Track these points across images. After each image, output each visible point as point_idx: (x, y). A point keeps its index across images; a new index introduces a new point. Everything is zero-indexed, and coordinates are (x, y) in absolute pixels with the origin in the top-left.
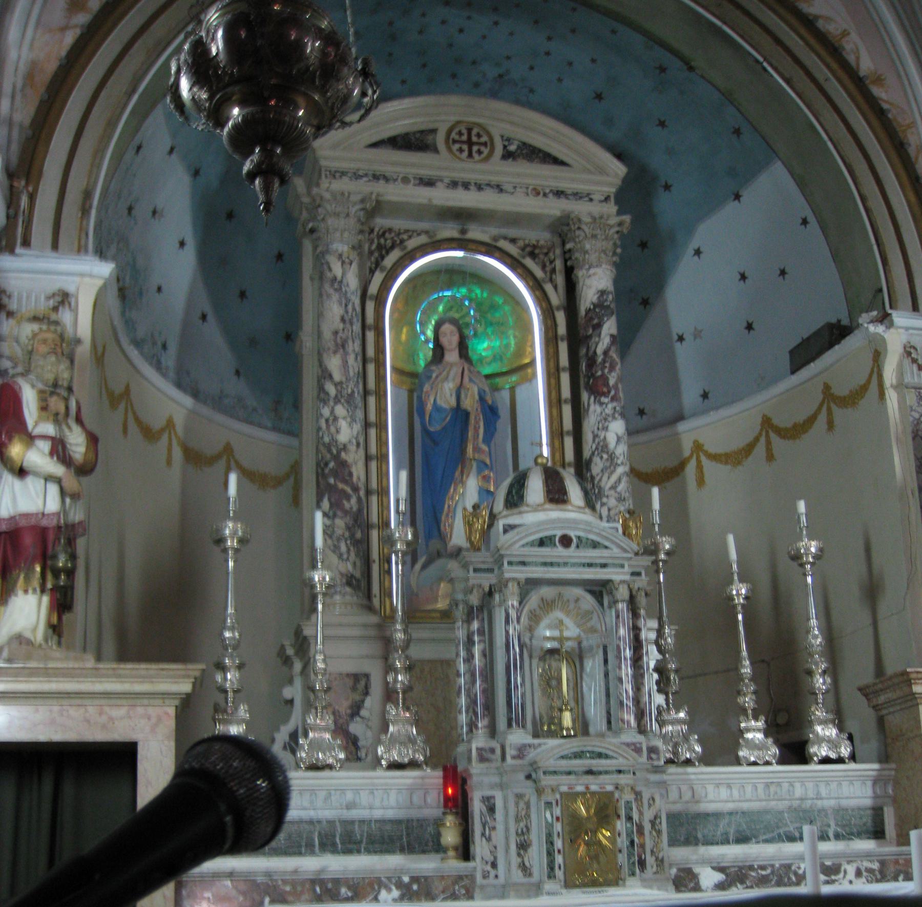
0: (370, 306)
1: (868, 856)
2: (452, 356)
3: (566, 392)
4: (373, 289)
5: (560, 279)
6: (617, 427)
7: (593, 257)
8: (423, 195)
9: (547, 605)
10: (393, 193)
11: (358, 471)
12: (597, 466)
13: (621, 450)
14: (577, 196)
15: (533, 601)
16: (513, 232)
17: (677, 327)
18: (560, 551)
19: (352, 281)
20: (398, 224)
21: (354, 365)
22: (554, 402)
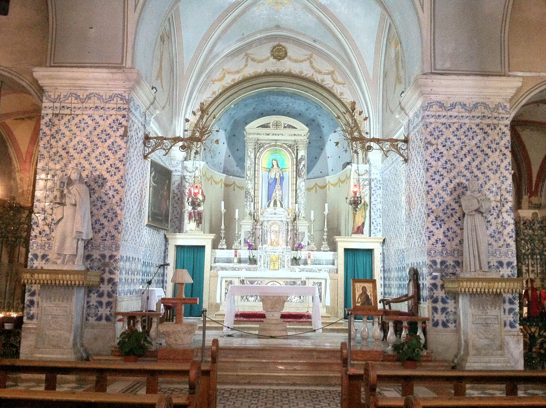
0: (257, 159)
1: (327, 268)
2: (275, 166)
3: (295, 176)
4: (257, 156)
5: (295, 152)
6: (303, 183)
7: (301, 148)
8: (267, 137)
9: (273, 224)
10: (260, 137)
11: (252, 193)
12: (298, 192)
13: (303, 188)
15: (270, 223)
16: (286, 142)
17: (328, 154)
18: (274, 215)
19: (253, 156)
20: (263, 142)
21: (252, 173)
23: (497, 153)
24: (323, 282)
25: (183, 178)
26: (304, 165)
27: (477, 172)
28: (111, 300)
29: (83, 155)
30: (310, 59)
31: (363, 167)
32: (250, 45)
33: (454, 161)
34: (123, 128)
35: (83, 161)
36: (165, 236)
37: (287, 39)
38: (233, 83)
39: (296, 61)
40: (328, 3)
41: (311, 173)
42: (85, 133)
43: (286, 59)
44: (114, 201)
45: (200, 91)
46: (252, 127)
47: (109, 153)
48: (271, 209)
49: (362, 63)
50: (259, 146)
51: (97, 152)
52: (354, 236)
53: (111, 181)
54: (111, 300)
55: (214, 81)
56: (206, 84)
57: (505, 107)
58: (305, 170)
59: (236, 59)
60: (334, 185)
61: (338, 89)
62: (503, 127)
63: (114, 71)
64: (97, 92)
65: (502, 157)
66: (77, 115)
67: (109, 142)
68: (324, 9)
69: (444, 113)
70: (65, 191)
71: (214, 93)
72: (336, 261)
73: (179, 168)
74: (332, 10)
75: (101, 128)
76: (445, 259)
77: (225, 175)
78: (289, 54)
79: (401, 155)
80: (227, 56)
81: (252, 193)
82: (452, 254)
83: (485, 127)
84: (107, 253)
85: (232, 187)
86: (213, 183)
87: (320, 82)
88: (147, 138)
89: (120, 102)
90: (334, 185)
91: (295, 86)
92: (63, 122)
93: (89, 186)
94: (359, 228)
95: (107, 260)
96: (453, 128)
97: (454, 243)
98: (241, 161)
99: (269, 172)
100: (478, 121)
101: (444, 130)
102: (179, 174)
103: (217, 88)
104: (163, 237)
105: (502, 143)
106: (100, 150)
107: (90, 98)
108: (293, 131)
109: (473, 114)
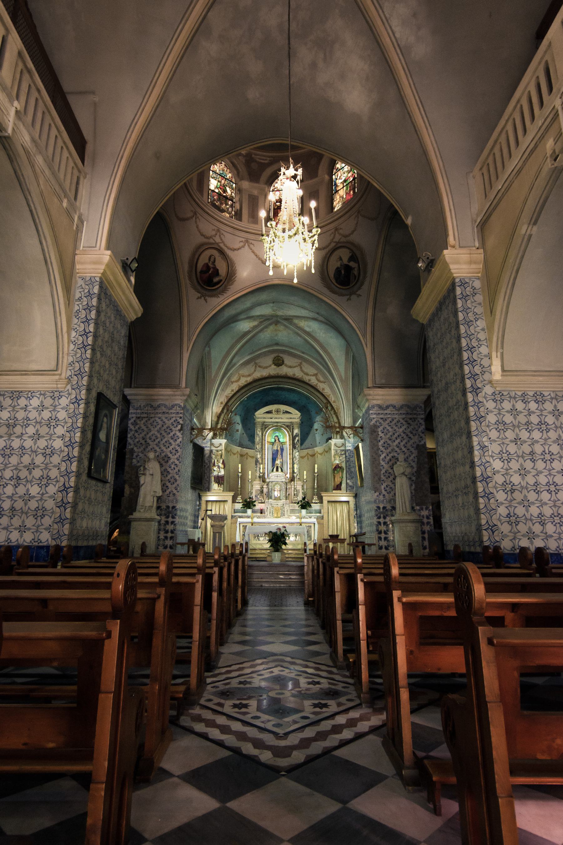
2: (277, 441)
6: (297, 453)
9: (276, 484)
10: (266, 420)
11: (260, 461)
13: (297, 457)
14: (293, 418)
15: (274, 483)
19: (260, 434)
21: (260, 446)
22: (290, 450)
23: (417, 437)
24: (312, 525)
25: (211, 451)
26: (298, 440)
27: (404, 449)
28: (173, 535)
29: (155, 443)
30: (300, 365)
31: (339, 441)
32: (259, 356)
33: (389, 442)
34: (180, 426)
35: (155, 446)
36: (199, 494)
37: (284, 352)
38: (246, 383)
39: (290, 367)
40: (311, 330)
41: (304, 445)
42: (156, 429)
43: (283, 366)
44: (175, 471)
45: (223, 390)
46: (260, 415)
47: (172, 441)
48: (275, 473)
49: (337, 369)
50: (265, 427)
51: (164, 441)
52: (334, 491)
53: (173, 459)
54: (173, 535)
55: (232, 382)
56: (227, 385)
57: (421, 407)
58: (299, 444)
59: (248, 366)
60: (321, 454)
61: (321, 386)
62: (420, 420)
63: (175, 390)
64: (164, 403)
65: (420, 439)
66: (152, 418)
67: (172, 434)
68: (308, 334)
69: (382, 412)
70: (146, 467)
71: (232, 391)
72: (322, 511)
73: (209, 444)
74: (314, 335)
75: (167, 425)
76: (385, 506)
77: (240, 448)
78: (285, 362)
79: (359, 436)
80: (242, 364)
81: (260, 461)
82: (390, 501)
83: (408, 420)
84: (171, 505)
85: (246, 456)
86: (232, 454)
87: (307, 381)
88: (192, 429)
89: (178, 409)
90: (321, 454)
91: (291, 384)
92: (142, 422)
93: (159, 462)
94: (337, 486)
95: (171, 509)
96: (388, 421)
97: (391, 495)
98: (252, 437)
99: (273, 445)
100: (404, 416)
101: (382, 422)
102: (209, 449)
103: (235, 387)
104: (197, 494)
105: (420, 430)
106: (166, 439)
107: (159, 407)
108: (288, 416)
109: (400, 412)
